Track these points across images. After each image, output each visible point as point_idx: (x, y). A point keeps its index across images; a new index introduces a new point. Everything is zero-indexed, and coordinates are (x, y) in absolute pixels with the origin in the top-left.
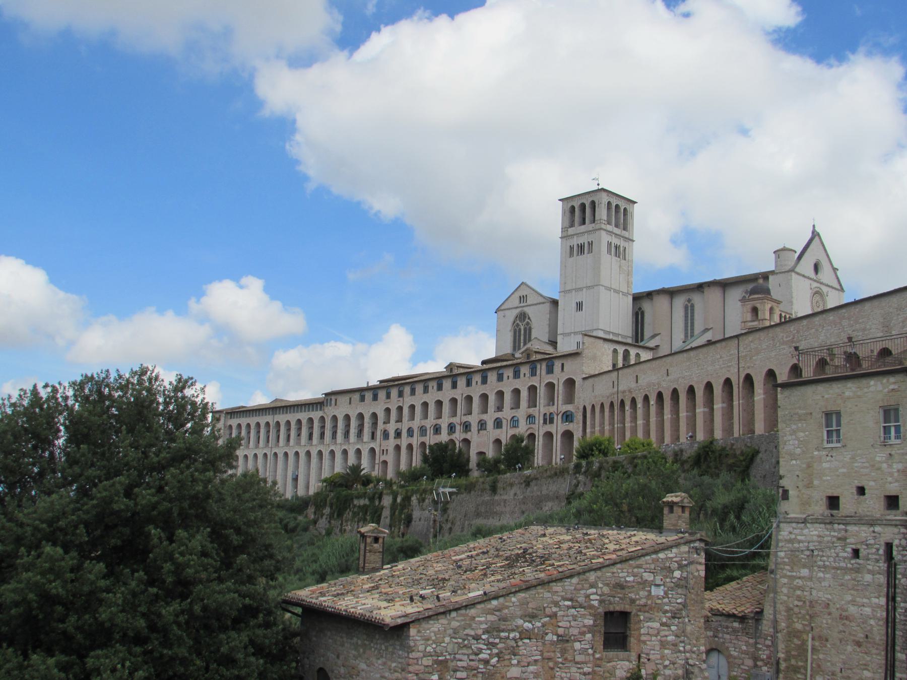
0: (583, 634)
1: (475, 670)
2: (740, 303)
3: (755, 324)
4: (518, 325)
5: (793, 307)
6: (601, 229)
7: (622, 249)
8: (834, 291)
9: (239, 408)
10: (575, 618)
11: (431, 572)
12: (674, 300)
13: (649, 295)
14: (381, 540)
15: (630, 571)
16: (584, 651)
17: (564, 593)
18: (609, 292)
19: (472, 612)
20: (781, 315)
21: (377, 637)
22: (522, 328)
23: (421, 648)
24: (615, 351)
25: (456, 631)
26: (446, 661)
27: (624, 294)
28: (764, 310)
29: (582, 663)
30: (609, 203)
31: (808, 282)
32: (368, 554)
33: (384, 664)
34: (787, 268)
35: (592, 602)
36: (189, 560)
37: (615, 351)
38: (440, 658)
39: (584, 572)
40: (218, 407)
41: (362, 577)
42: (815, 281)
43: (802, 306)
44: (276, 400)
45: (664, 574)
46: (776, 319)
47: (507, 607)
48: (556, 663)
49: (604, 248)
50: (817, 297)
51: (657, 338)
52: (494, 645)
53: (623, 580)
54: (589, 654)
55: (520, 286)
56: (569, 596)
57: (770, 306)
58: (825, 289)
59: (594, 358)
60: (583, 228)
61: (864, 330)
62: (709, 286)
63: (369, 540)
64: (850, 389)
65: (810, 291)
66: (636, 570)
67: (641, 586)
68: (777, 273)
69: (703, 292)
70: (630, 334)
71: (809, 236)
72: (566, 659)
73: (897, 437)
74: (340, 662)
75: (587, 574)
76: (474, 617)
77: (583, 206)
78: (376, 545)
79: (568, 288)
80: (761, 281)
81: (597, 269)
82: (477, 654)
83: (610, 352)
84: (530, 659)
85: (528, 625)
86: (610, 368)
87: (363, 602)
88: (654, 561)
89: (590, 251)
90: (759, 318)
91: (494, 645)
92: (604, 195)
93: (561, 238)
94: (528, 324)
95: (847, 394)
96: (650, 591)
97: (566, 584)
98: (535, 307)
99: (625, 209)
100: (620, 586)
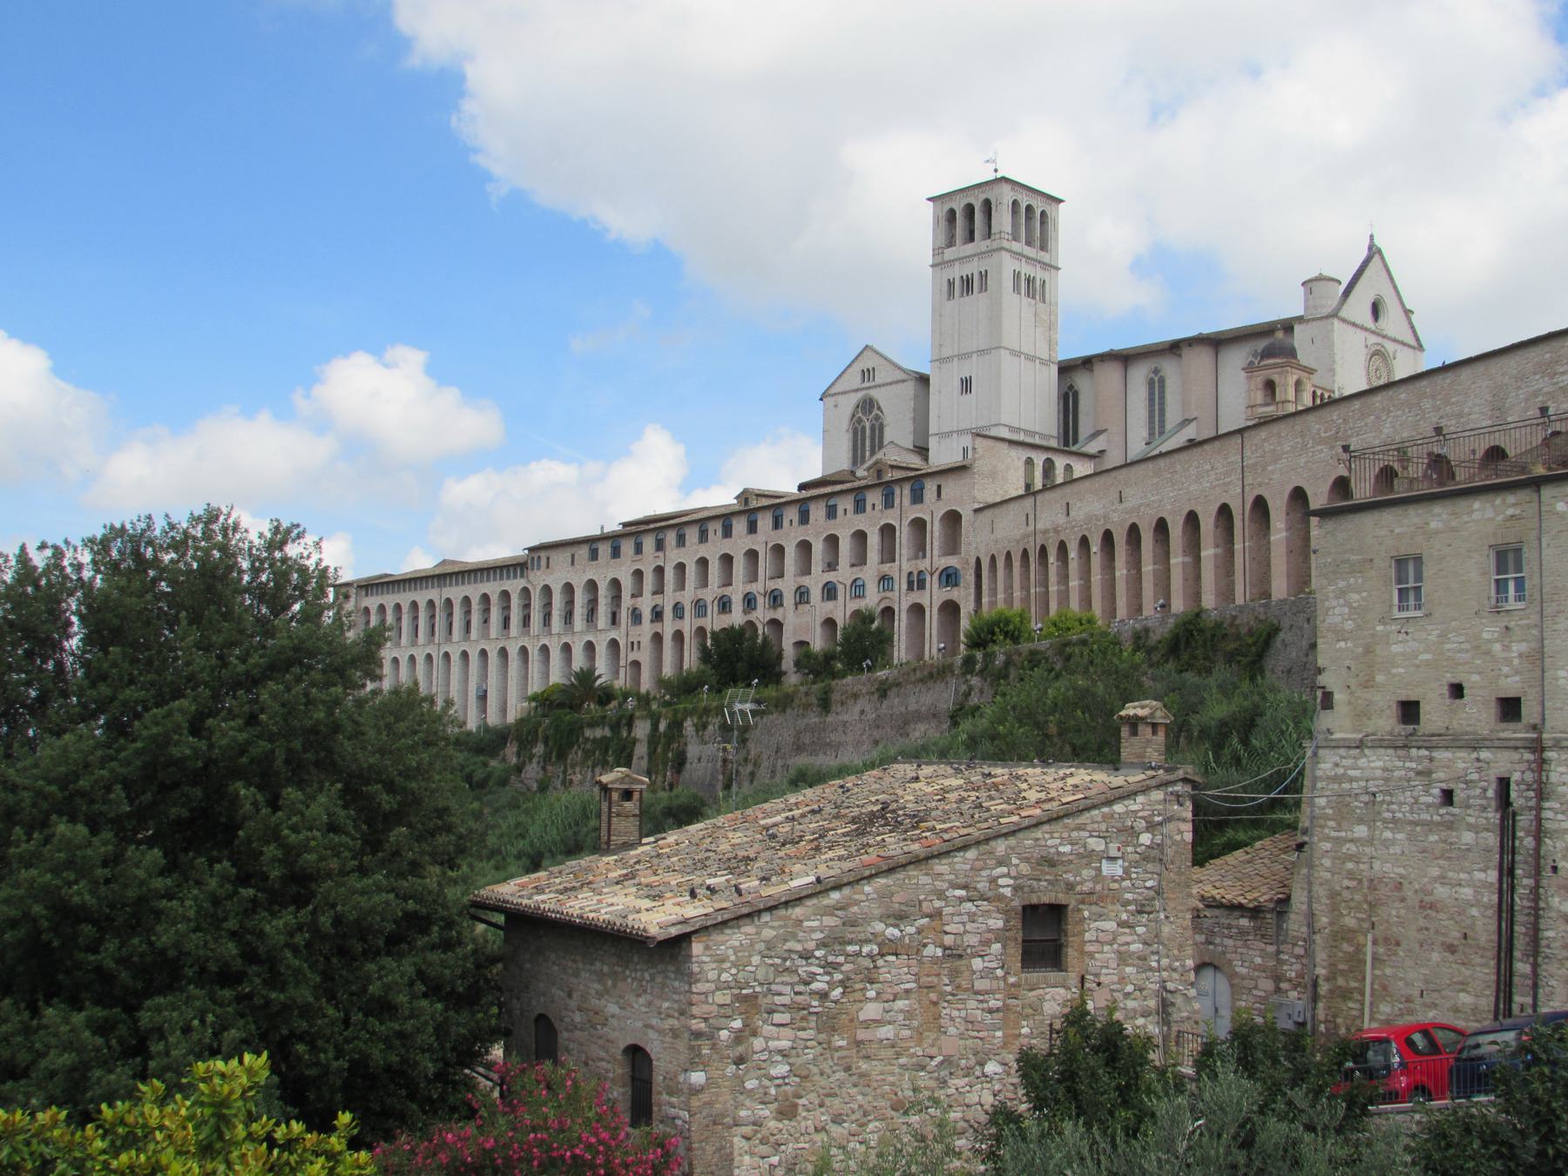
0: (987, 943)
1: (804, 1009)
2: (1243, 374)
3: (1270, 409)
4: (860, 421)
5: (1337, 378)
6: (1001, 249)
7: (1038, 283)
9: (381, 577)
10: (972, 918)
11: (724, 846)
13: (1087, 363)
14: (636, 796)
15: (1065, 835)
16: (988, 973)
17: (953, 877)
18: (1017, 359)
19: (797, 912)
20: (1314, 392)
21: (636, 959)
22: (868, 425)
23: (712, 975)
24: (1029, 462)
25: (770, 946)
26: (755, 996)
27: (1044, 363)
28: (1285, 386)
29: (987, 993)
30: (1015, 203)
31: (1361, 335)
32: (614, 820)
33: (650, 1004)
34: (1326, 311)
35: (1001, 890)
36: (308, 839)
37: (1029, 462)
38: (744, 992)
39: (987, 840)
40: (346, 576)
41: (606, 859)
42: (1373, 332)
43: (1351, 379)
44: (444, 562)
45: (1123, 839)
46: (1307, 401)
47: (857, 903)
48: (942, 994)
49: (1008, 283)
50: (1377, 361)
51: (1102, 438)
52: (836, 966)
53: (1053, 850)
54: (997, 978)
55: (862, 352)
56: (961, 881)
57: (1295, 377)
58: (1390, 347)
59: (993, 475)
60: (970, 248)
61: (1460, 415)
62: (1190, 345)
63: (615, 796)
64: (1438, 517)
65: (1365, 351)
66: (1074, 834)
67: (1085, 861)
68: (1308, 321)
69: (1180, 356)
70: (1055, 434)
71: (1364, 254)
72: (958, 987)
73: (1519, 598)
74: (573, 1004)
75: (993, 843)
76: (801, 921)
77: (970, 210)
78: (627, 804)
79: (946, 352)
80: (1280, 335)
81: (995, 319)
82: (807, 983)
83: (1021, 464)
84: (897, 989)
85: (892, 932)
86: (1021, 492)
87: (610, 901)
88: (1104, 816)
89: (984, 287)
90: (1278, 399)
91: (836, 966)
92: (1006, 188)
93: (932, 266)
94: (877, 418)
95: (1434, 525)
96: (1099, 869)
97: (956, 860)
98: (889, 388)
99: (1043, 214)
100: (1050, 862)
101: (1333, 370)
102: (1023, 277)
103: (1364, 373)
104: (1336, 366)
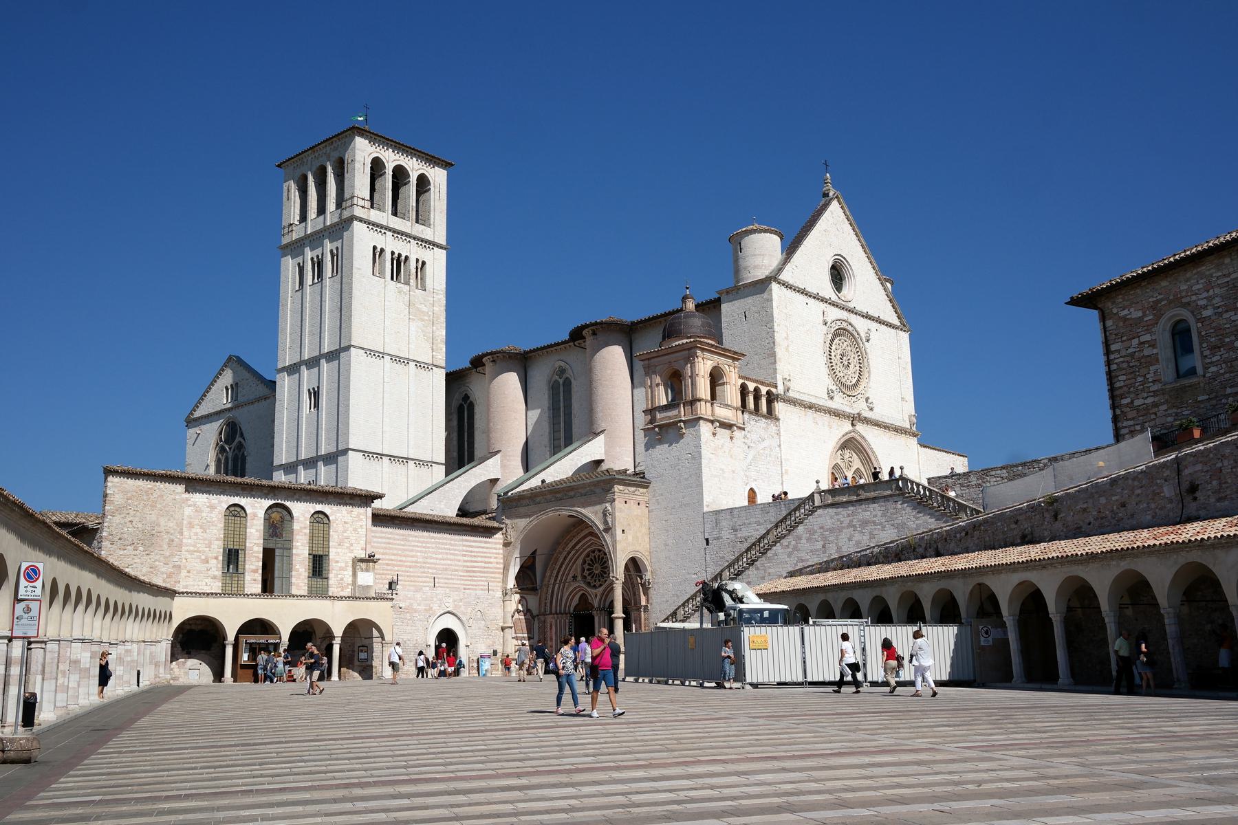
5: (779, 366)
6: (353, 218)
7: (413, 264)
8: (884, 327)
12: (530, 373)
13: (477, 363)
24: (236, 512)
34: (761, 274)
37: (236, 512)
50: (842, 345)
58: (861, 325)
59: (147, 539)
62: (594, 334)
70: (442, 459)
94: (240, 446)
101: (773, 355)
102: (388, 256)
103: (823, 359)
104: (777, 350)
